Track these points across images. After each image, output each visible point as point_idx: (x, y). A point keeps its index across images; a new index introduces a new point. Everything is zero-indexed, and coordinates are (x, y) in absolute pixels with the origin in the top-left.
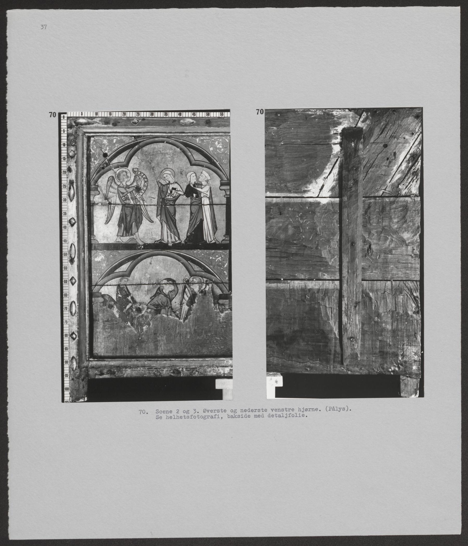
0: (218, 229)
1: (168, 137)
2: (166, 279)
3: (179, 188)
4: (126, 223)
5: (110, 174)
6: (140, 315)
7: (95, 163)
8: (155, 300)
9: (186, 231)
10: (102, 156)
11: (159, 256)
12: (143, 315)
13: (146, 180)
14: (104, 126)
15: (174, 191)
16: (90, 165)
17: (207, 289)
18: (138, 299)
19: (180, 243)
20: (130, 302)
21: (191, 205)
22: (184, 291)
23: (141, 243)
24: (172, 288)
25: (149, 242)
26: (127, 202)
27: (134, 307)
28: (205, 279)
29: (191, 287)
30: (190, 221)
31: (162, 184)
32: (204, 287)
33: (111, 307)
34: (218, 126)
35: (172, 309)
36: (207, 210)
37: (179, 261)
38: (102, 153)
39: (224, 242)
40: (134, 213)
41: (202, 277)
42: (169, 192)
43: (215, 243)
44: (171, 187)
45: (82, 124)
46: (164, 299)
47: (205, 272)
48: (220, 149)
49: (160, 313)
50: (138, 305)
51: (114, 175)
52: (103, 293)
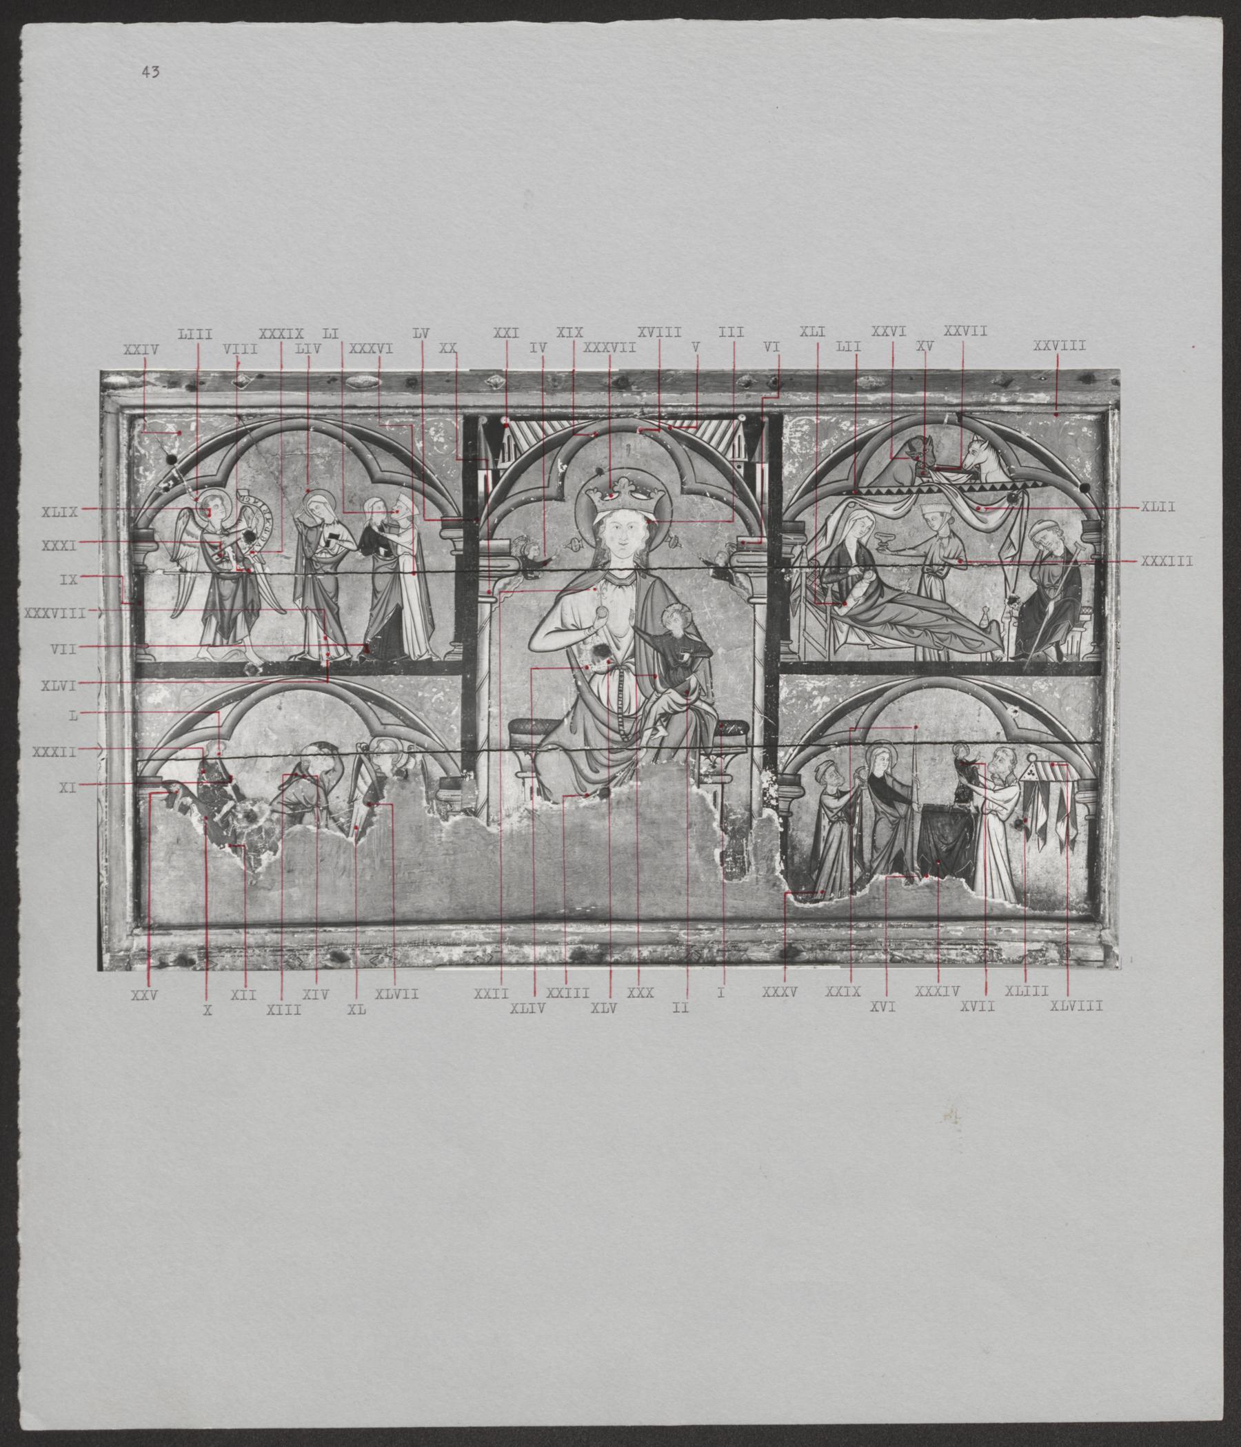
0: (437, 628)
1: (317, 417)
2: (315, 744)
3: (345, 535)
4: (223, 615)
5: (186, 501)
6: (255, 826)
7: (150, 478)
8: (292, 794)
9: (364, 631)
10: (163, 461)
11: (300, 691)
12: (260, 828)
13: (268, 516)
14: (166, 390)
15: (333, 541)
16: (136, 482)
17: (410, 766)
18: (247, 791)
19: (348, 660)
20: (231, 799)
21: (374, 573)
22: (357, 771)
23: (257, 662)
24: (329, 763)
25: (277, 657)
26: (225, 566)
27: (239, 808)
28: (407, 744)
29: (375, 761)
30: (372, 609)
31: (305, 526)
32: (403, 761)
33: (185, 809)
34: (436, 391)
35: (330, 813)
36: (411, 585)
37: (346, 701)
38: (165, 456)
39: (450, 658)
40: (240, 593)
41: (399, 738)
42: (323, 543)
43: (429, 661)
44: (327, 532)
45: (115, 387)
46: (311, 790)
47: (408, 726)
48: (440, 445)
49: (300, 822)
50: (248, 805)
51: (192, 505)
52: (165, 778)
